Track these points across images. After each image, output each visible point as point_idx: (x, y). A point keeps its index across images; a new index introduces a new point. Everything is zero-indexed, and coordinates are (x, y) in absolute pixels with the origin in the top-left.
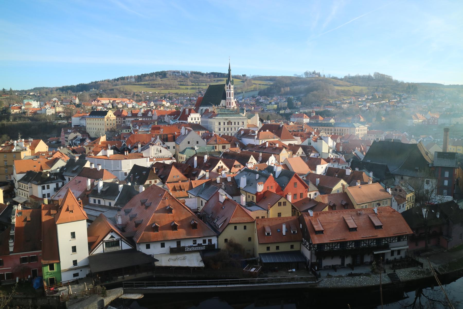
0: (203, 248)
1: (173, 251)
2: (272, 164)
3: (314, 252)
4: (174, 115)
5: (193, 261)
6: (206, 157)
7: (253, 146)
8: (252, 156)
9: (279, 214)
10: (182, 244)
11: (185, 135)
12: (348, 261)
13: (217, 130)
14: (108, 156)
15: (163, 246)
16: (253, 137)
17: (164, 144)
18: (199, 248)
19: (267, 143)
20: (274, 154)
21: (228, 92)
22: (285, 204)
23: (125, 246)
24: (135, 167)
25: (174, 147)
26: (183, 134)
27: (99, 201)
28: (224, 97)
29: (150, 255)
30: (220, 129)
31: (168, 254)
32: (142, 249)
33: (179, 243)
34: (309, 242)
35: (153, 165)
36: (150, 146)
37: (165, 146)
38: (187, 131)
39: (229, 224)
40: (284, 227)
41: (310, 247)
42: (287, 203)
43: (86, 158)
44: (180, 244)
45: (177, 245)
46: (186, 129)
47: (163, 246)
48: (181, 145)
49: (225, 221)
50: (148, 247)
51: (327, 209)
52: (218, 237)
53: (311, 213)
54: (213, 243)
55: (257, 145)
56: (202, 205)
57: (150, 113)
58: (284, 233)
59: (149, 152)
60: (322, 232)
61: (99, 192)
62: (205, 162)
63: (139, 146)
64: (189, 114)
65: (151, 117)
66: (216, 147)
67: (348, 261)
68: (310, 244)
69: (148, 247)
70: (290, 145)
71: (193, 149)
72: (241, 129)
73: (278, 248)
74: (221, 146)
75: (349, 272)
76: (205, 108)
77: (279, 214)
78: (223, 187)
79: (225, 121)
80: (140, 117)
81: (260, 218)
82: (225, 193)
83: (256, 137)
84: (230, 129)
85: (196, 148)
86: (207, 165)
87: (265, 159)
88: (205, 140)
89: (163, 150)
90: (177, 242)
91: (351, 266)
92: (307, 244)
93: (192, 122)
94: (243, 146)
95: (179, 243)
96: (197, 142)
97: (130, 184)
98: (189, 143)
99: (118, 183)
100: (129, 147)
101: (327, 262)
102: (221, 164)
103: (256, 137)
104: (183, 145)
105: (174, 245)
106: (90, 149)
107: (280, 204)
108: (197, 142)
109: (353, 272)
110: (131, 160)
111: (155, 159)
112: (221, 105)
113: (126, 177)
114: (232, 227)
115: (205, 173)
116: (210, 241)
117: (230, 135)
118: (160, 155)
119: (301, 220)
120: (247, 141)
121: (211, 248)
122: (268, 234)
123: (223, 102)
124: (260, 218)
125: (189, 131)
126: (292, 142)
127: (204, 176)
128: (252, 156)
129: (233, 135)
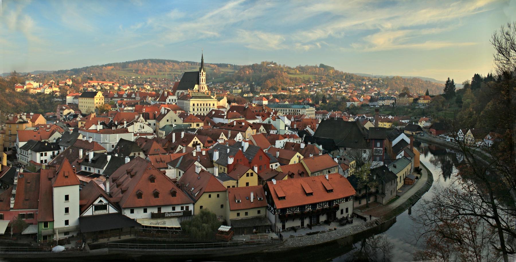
0: (181, 214)
1: (153, 216)
2: (240, 140)
3: (277, 216)
4: (154, 97)
5: (174, 224)
6: (183, 134)
7: (223, 124)
8: (222, 133)
9: (247, 184)
10: (163, 211)
11: (165, 115)
12: (307, 222)
13: (191, 110)
14: (98, 130)
15: (145, 211)
16: (222, 117)
17: (146, 121)
18: (178, 214)
19: (235, 122)
20: (241, 131)
21: (201, 78)
22: (252, 175)
24: (121, 140)
25: (154, 124)
26: (163, 113)
28: (198, 84)
29: (134, 220)
30: (194, 110)
31: (149, 219)
32: (127, 213)
33: (159, 210)
34: (273, 207)
35: (136, 140)
36: (135, 123)
37: (147, 123)
38: (166, 110)
39: (204, 192)
40: (252, 195)
41: (275, 212)
42: (254, 174)
43: (79, 132)
44: (160, 211)
45: (158, 211)
46: (165, 109)
47: (145, 211)
48: (161, 122)
49: (201, 190)
50: (132, 212)
51: (286, 178)
52: (194, 204)
53: (274, 181)
54: (190, 210)
55: (226, 124)
56: (180, 175)
57: (133, 95)
58: (252, 200)
60: (284, 198)
61: (90, 160)
62: (182, 137)
63: (125, 122)
64: (168, 96)
65: (134, 98)
66: (191, 125)
67: (307, 222)
68: (274, 209)
69: (132, 212)
70: (254, 123)
71: (172, 125)
72: (213, 110)
73: (246, 214)
74: (195, 124)
75: (309, 231)
76: (181, 91)
77: (247, 184)
78: (199, 160)
80: (125, 98)
81: (231, 187)
82: (200, 165)
83: (225, 117)
84: (202, 110)
85: (174, 126)
87: (234, 136)
89: (146, 127)
90: (158, 209)
91: (310, 226)
92: (272, 209)
93: (170, 103)
94: (214, 125)
95: (159, 210)
96: (175, 121)
97: (117, 155)
98: (168, 121)
99: (106, 154)
100: (116, 123)
101: (288, 225)
102: (196, 139)
103: (225, 117)
104: (163, 123)
105: (156, 211)
106: (82, 123)
107: (248, 175)
108: (175, 121)
109: (312, 231)
110: (118, 135)
111: (138, 135)
112: (195, 89)
113: (113, 149)
114: (206, 196)
115: (182, 147)
116: (187, 208)
117: (202, 115)
118: (143, 131)
119: (266, 188)
120: (217, 120)
121: (187, 213)
122: (239, 201)
123: (196, 86)
124: (231, 187)
125: (168, 111)
126: (255, 121)
127: (181, 151)
128: (222, 133)
129: (205, 114)
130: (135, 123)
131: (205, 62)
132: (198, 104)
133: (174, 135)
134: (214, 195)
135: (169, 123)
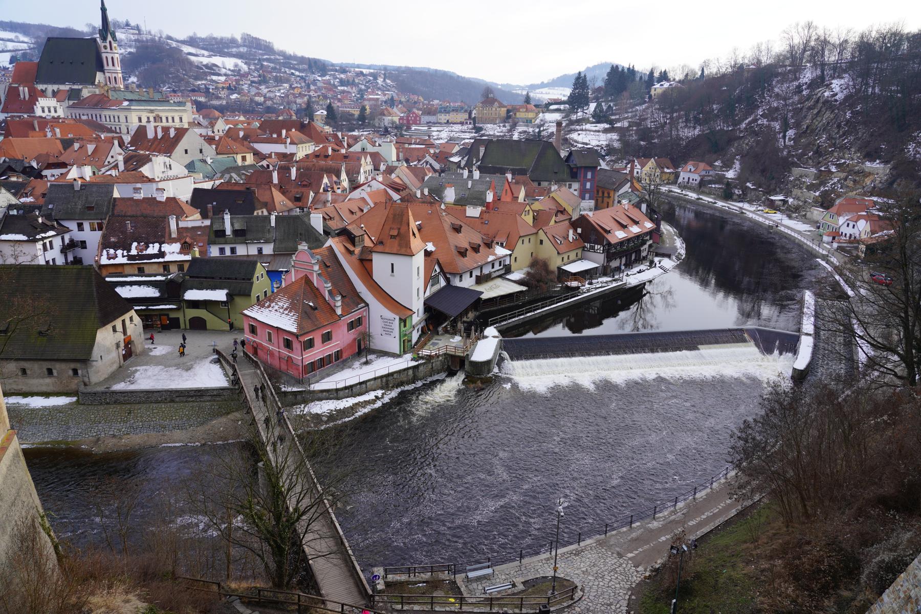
14: (88, 179)
15: (471, 276)
19: (330, 149)
23: (443, 283)
27: (233, 250)
32: (456, 282)
47: (471, 276)
50: (461, 280)
55: (293, 155)
59: (152, 169)
61: (229, 232)
62: (293, 177)
71: (204, 161)
79: (149, 115)
85: (209, 161)
86: (305, 183)
88: (214, 146)
93: (44, 115)
98: (186, 151)
102: (325, 180)
108: (201, 151)
118: (170, 173)
130: (154, 158)
131: (111, 17)
132: (167, 118)
133: (275, 175)
134: (526, 240)
135: (195, 156)
